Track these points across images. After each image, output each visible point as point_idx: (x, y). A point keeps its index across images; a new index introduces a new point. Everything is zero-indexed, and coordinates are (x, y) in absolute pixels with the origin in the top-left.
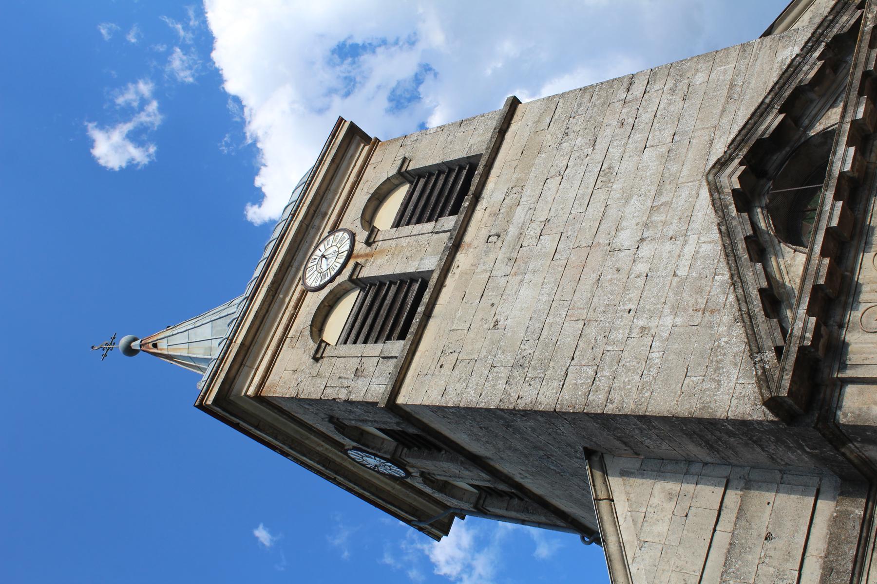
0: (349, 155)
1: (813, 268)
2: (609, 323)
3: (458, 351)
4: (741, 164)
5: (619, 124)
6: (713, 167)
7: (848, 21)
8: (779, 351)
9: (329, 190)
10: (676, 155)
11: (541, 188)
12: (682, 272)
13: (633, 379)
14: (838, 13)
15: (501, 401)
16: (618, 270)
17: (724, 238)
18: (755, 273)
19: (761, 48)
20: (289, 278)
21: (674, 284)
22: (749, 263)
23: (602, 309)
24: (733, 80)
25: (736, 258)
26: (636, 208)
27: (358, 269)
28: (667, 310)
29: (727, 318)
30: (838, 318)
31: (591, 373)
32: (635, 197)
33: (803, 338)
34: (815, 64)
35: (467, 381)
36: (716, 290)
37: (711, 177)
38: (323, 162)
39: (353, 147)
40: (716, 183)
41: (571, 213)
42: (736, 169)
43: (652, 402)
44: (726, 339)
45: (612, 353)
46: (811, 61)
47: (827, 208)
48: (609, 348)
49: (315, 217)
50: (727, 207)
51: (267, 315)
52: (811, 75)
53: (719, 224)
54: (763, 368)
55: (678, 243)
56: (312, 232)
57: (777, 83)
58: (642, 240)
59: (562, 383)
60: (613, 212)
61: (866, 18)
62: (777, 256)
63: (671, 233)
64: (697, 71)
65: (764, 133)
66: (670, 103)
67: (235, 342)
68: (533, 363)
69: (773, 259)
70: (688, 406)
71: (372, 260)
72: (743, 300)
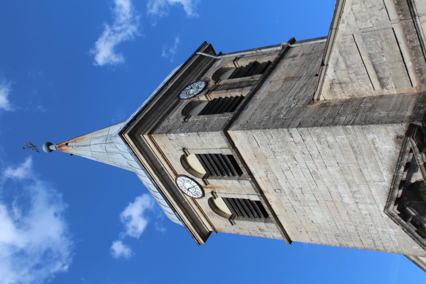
4: (395, 205)
5: (302, 154)
9: (152, 160)
14: (402, 156)
17: (408, 233)
25: (417, 238)
26: (343, 190)
27: (214, 194)
28: (388, 227)
37: (386, 212)
39: (139, 140)
40: (390, 213)
49: (160, 172)
51: (187, 210)
53: (403, 229)
56: (166, 177)
61: (418, 160)
63: (369, 203)
64: (326, 136)
66: (323, 149)
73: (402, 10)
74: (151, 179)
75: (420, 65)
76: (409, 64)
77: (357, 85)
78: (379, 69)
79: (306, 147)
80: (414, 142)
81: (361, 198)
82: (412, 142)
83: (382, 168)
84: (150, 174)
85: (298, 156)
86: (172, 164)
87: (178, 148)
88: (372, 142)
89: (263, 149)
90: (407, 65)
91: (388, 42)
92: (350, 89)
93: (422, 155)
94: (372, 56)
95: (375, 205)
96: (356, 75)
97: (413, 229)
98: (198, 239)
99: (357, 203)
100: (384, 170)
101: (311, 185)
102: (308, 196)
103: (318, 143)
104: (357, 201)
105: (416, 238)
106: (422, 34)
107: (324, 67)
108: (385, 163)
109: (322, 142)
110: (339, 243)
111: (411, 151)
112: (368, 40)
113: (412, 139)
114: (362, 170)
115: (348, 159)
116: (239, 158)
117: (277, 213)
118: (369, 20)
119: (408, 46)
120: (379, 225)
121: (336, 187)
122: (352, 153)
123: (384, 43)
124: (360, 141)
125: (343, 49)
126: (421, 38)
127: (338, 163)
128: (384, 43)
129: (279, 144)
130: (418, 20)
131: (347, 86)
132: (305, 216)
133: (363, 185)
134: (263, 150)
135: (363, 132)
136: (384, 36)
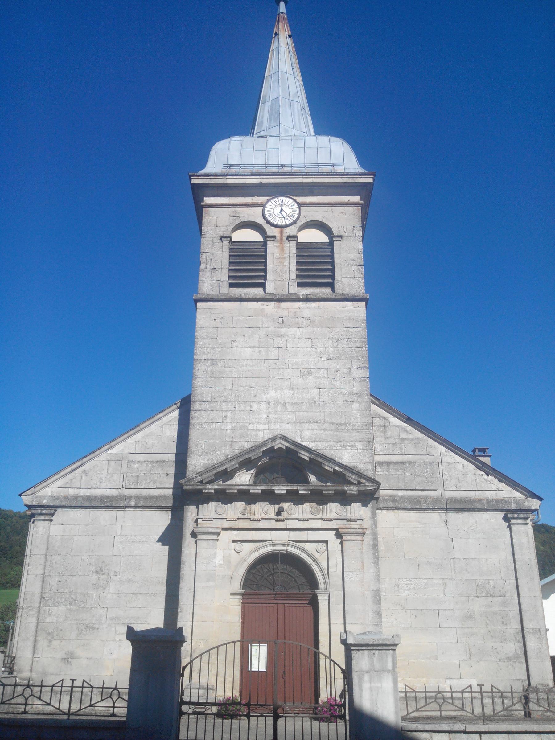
1: (233, 487)
2: (230, 400)
3: (222, 326)
4: (286, 447)
5: (337, 370)
6: (284, 436)
7: (352, 478)
8: (201, 482)
10: (312, 406)
11: (307, 337)
12: (251, 427)
13: (204, 419)
15: (197, 360)
16: (255, 396)
18: (235, 465)
19: (366, 433)
21: (245, 424)
22: (238, 462)
23: (237, 394)
24: (349, 424)
26: (286, 394)
27: (272, 239)
28: (233, 425)
29: (228, 452)
31: (208, 399)
32: (292, 392)
33: (205, 489)
34: (332, 468)
35: (208, 337)
36: (240, 444)
38: (343, 176)
41: (289, 360)
42: (284, 445)
43: (195, 430)
44: (219, 453)
45: (216, 406)
46: (333, 466)
47: (258, 488)
48: (218, 404)
52: (327, 468)
54: (193, 478)
55: (265, 421)
57: (323, 455)
58: (269, 403)
59: (204, 387)
60: (287, 383)
61: (351, 486)
63: (270, 416)
64: (360, 403)
65: (300, 453)
66: (344, 394)
67: (227, 178)
68: (214, 369)
70: (192, 446)
71: (278, 245)
72: (222, 464)
74: (307, 173)
76: (401, 493)
77: (382, 441)
79: (344, 377)
80: (372, 488)
81: (276, 409)
82: (371, 486)
83: (320, 444)
84: (313, 176)
85: (332, 364)
86: (316, 207)
88: (352, 445)
91: (425, 482)
92: (378, 434)
93: (355, 491)
94: (412, 465)
95: (267, 422)
96: (393, 444)
98: (200, 177)
99: (269, 403)
100: (317, 445)
103: (350, 392)
104: (272, 404)
106: (430, 511)
108: (326, 449)
109: (352, 397)
111: (359, 483)
113: (375, 487)
114: (316, 424)
118: (447, 474)
119: (423, 497)
120: (236, 416)
121: (291, 389)
122: (339, 421)
123: (424, 479)
124: (353, 434)
125: (421, 442)
127: (324, 402)
128: (424, 479)
129: (349, 351)
130: (443, 512)
131: (382, 432)
132: (243, 337)
133: (295, 418)
134: (340, 330)
135: (365, 441)
136: (431, 481)
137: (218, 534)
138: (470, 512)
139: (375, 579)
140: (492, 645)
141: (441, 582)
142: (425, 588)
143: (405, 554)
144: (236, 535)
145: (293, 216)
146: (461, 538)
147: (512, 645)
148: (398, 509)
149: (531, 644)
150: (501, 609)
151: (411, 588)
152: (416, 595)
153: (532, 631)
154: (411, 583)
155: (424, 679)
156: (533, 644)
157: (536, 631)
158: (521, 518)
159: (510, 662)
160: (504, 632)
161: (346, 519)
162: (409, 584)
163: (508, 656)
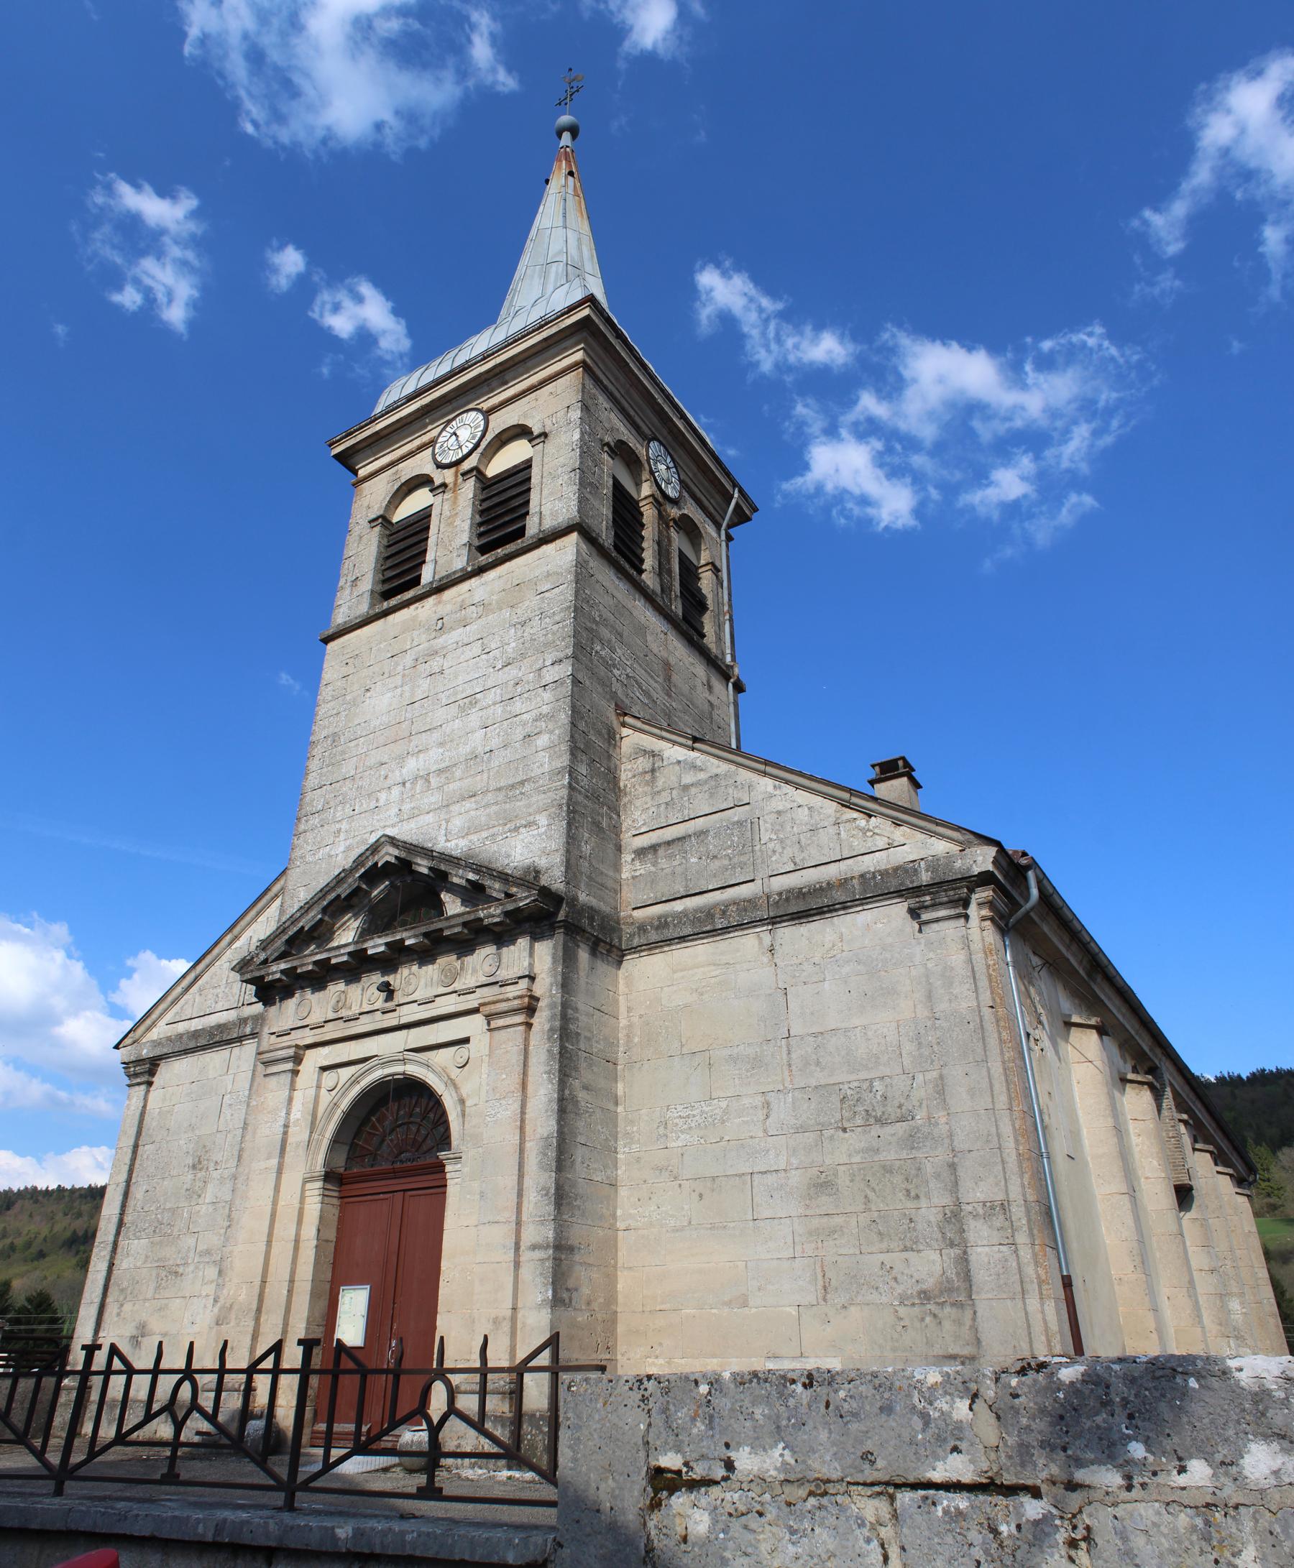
0: (563, 345)
5: (516, 680)
8: (265, 962)
18: (315, 916)
20: (443, 411)
26: (433, 758)
27: (441, 490)
28: (348, 843)
30: (303, 985)
33: (268, 975)
37: (383, 839)
50: (363, 866)
53: (344, 870)
56: (486, 389)
61: (490, 907)
62: (354, 916)
63: (403, 808)
64: (551, 732)
66: (524, 724)
69: (350, 915)
73: (787, 899)
75: (675, 925)
76: (678, 906)
78: (674, 849)
80: (528, 901)
82: (526, 898)
83: (474, 837)
85: (512, 672)
87: (548, 422)
89: (531, 603)
90: (678, 901)
93: (498, 916)
96: (667, 804)
97: (343, 891)
99: (404, 784)
100: (470, 841)
101: (447, 693)
102: (424, 685)
104: (408, 785)
105: (324, 896)
106: (736, 934)
107: (690, 743)
109: (538, 723)
110: (318, 741)
111: (508, 895)
112: (736, 832)
114: (473, 799)
115: (498, 771)
116: (517, 550)
117: (391, 618)
118: (775, 837)
119: (716, 905)
121: (441, 744)
123: (726, 862)
124: (534, 799)
126: (729, 933)
128: (726, 862)
130: (765, 928)
131: (647, 783)
136: (740, 862)
137: (298, 1059)
138: (827, 915)
139: (547, 1111)
140: (882, 1257)
141: (759, 1100)
142: (723, 1122)
143: (682, 1046)
144: (326, 1056)
145: (473, 438)
146: (805, 983)
147: (935, 1256)
148: (669, 941)
149: (979, 1249)
150: (904, 1155)
151: (693, 1125)
152: (702, 1141)
153: (981, 1211)
154: (694, 1113)
155: (715, 1361)
156: (987, 1249)
157: (992, 1208)
158: (941, 904)
159: (929, 1307)
160: (911, 1220)
161: (497, 983)
162: (688, 1117)
163: (924, 1287)
